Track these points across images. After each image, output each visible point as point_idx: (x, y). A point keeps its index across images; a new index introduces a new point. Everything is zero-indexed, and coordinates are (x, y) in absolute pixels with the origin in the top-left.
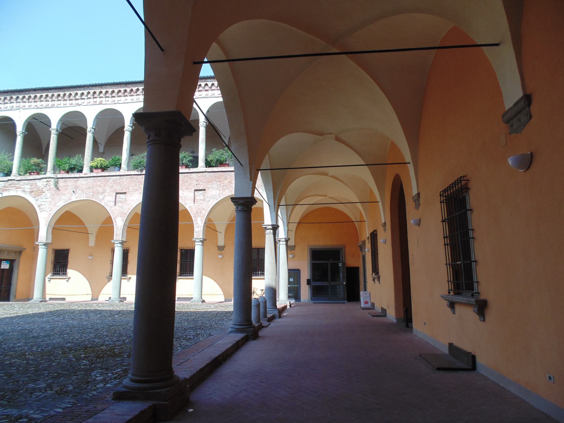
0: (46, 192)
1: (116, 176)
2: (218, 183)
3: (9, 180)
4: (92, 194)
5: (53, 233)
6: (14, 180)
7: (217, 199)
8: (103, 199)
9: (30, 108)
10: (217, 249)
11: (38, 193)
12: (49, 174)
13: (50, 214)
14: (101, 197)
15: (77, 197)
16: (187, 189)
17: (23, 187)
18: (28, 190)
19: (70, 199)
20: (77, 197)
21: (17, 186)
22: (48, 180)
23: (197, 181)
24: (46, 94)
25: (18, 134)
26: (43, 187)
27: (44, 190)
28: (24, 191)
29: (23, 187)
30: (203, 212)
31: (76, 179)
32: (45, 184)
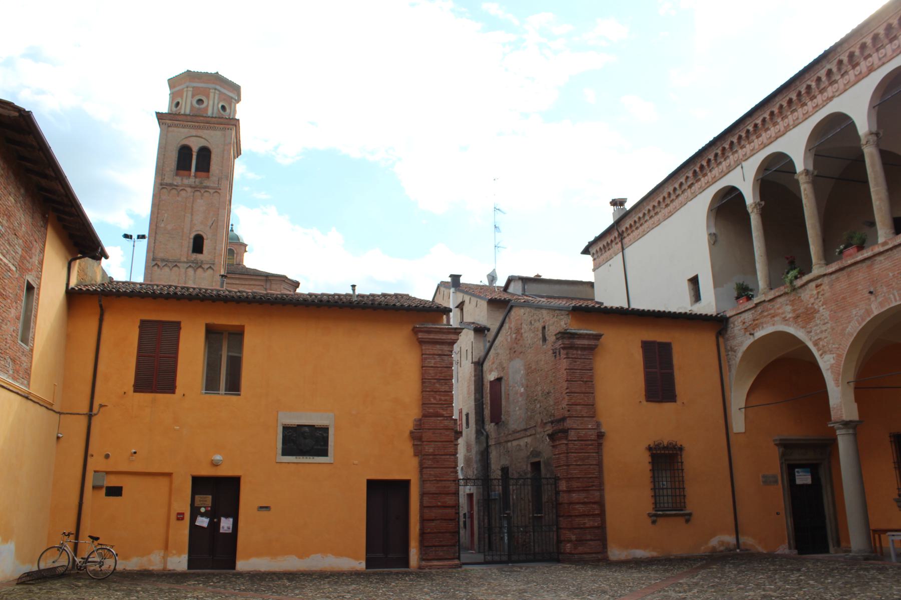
3: (757, 305)
5: (857, 399)
6: (764, 301)
9: (754, 152)
11: (806, 316)
12: (816, 271)
13: (839, 356)
15: (881, 304)
17: (780, 311)
18: (791, 315)
19: (868, 312)
20: (881, 304)
21: (772, 311)
22: (819, 281)
24: (768, 112)
25: (750, 210)
26: (812, 300)
27: (816, 307)
29: (780, 311)
31: (868, 263)
32: (815, 292)
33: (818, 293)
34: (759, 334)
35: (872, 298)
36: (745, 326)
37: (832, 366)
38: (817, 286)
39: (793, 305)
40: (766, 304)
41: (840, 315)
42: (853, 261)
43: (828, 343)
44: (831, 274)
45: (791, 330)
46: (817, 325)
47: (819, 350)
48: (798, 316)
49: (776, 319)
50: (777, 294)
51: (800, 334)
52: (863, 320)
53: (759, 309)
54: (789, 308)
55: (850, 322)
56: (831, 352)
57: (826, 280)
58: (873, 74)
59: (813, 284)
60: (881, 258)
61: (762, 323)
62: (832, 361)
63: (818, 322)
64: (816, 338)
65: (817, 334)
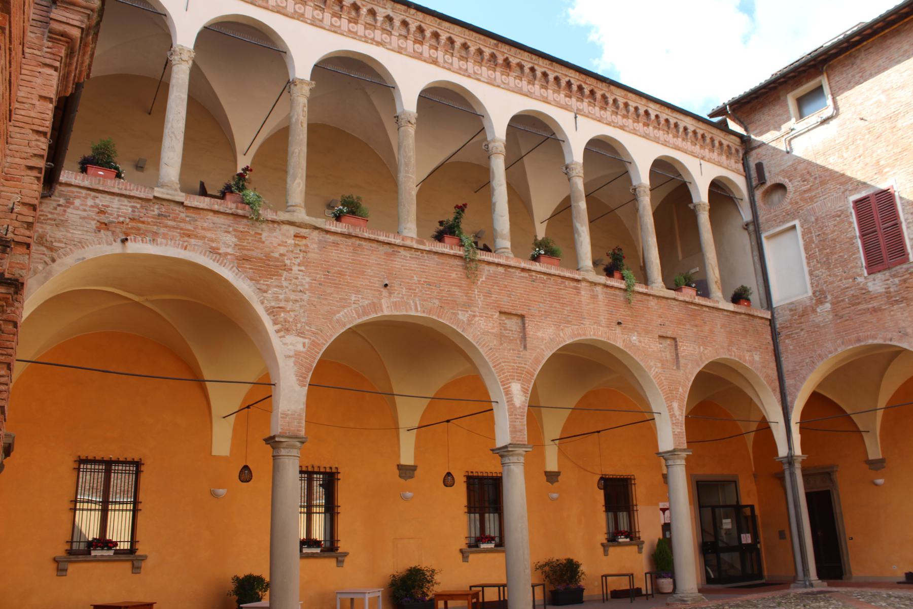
0: (295, 269)
1: (498, 265)
2: (695, 330)
4: (437, 302)
7: (698, 365)
8: (469, 323)
10: (545, 478)
13: (314, 344)
14: (463, 316)
16: (647, 332)
17: (209, 235)
18: (230, 250)
19: (375, 307)
20: (395, 304)
22: (303, 231)
23: (660, 317)
26: (282, 250)
27: (288, 262)
28: (214, 251)
29: (209, 235)
30: (681, 390)
33: (296, 245)
34: (137, 247)
35: (385, 292)
36: (103, 218)
37: (297, 354)
38: (296, 236)
39: (240, 239)
40: (178, 209)
41: (329, 290)
42: (372, 236)
43: (296, 321)
44: (328, 232)
45: (227, 273)
46: (281, 287)
47: (275, 323)
48: (246, 259)
49: (193, 241)
50: (216, 207)
51: (244, 286)
52: (365, 313)
53: (156, 210)
54: (231, 239)
55: (344, 307)
56: (300, 334)
57: (315, 235)
58: (433, 67)
59: (292, 230)
60: (407, 254)
61: (155, 234)
62: (300, 348)
63: (285, 284)
64: (273, 304)
65: (277, 299)
